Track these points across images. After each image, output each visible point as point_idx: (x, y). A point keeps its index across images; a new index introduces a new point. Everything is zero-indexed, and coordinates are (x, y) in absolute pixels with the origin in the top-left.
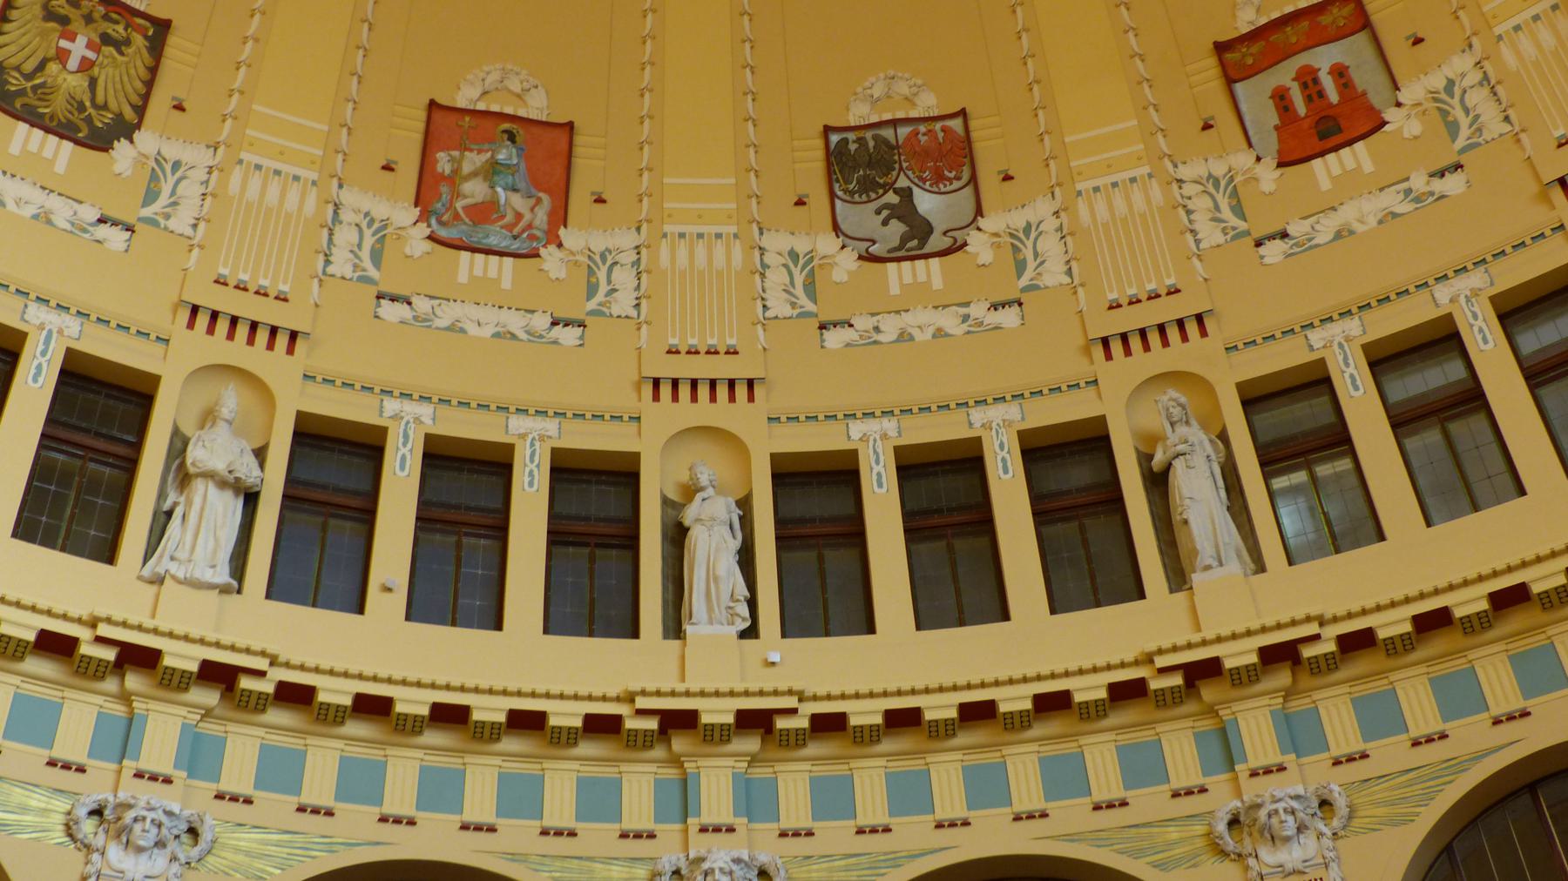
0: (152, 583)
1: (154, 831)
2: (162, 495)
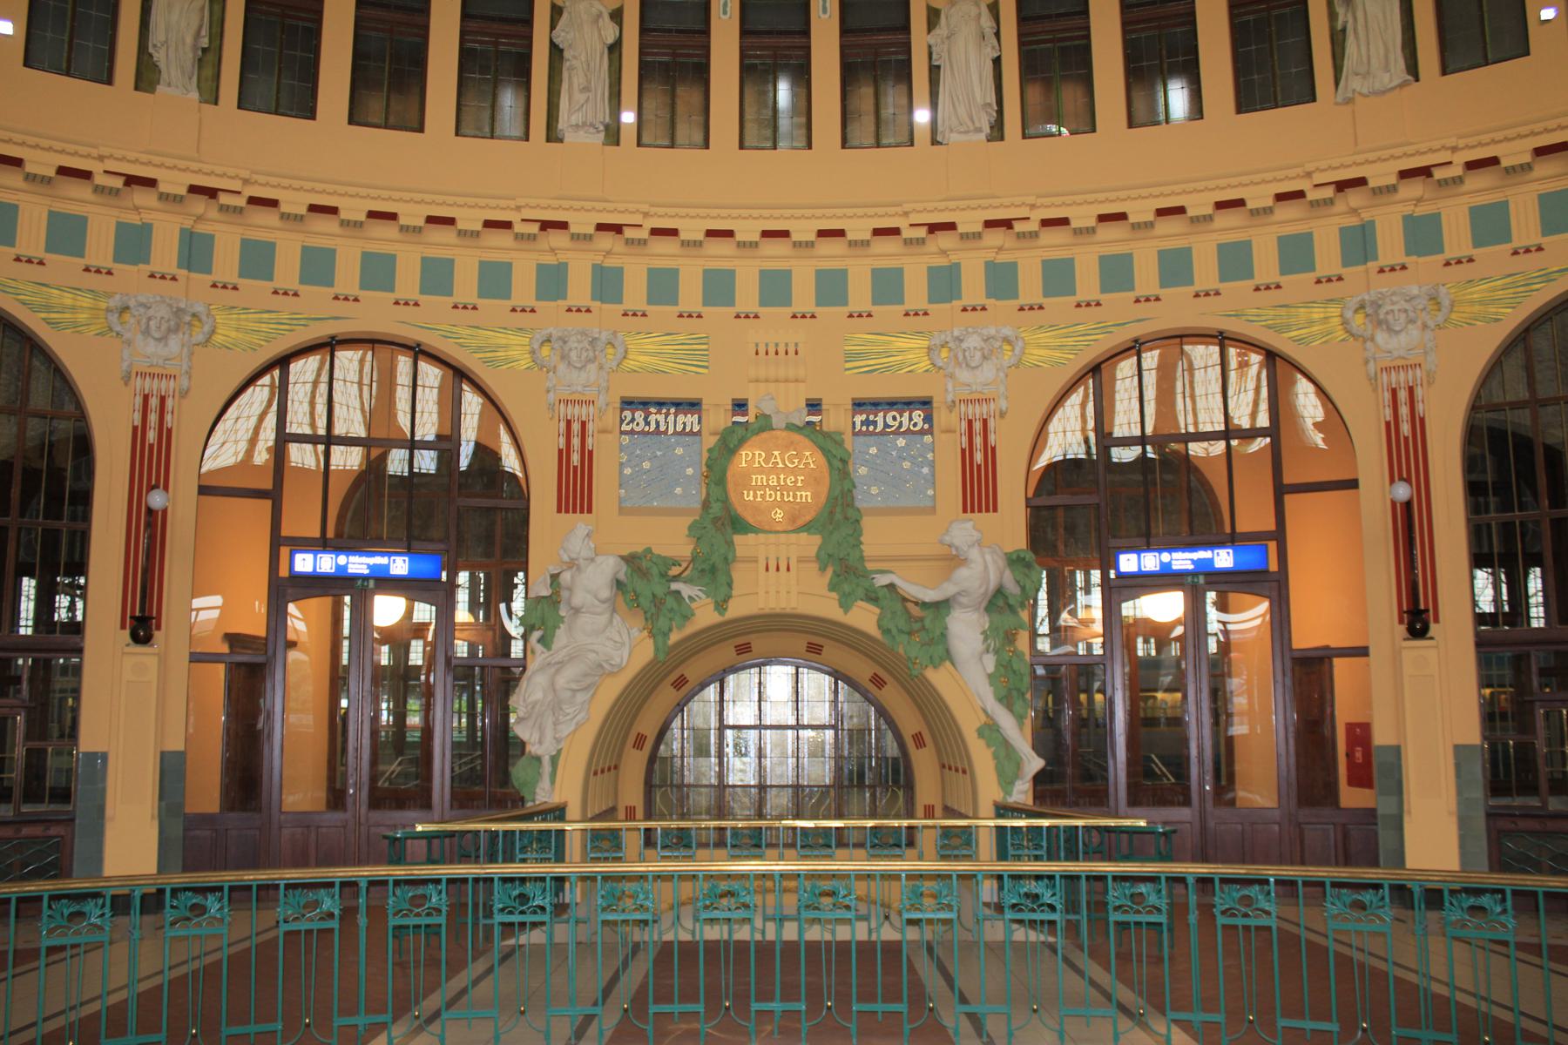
0: (1347, 103)
1: (1403, 316)
2: (1332, 16)
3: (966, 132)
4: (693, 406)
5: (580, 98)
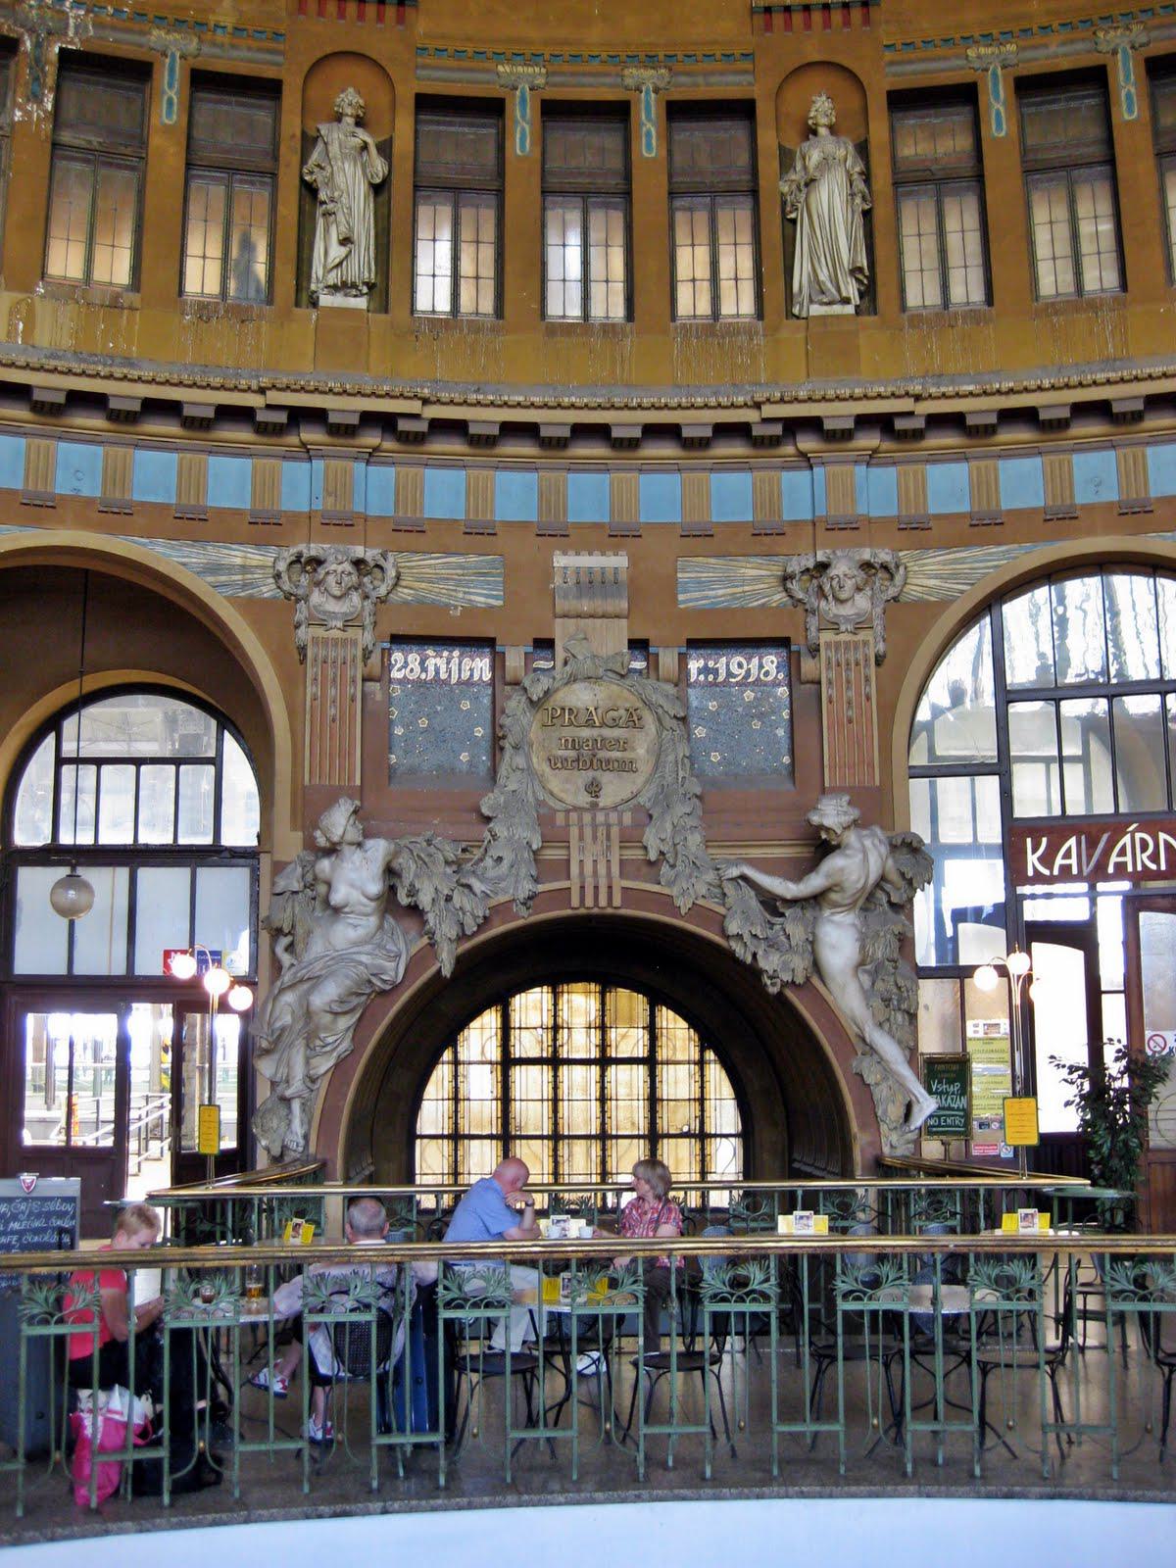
3: (829, 303)
5: (337, 252)
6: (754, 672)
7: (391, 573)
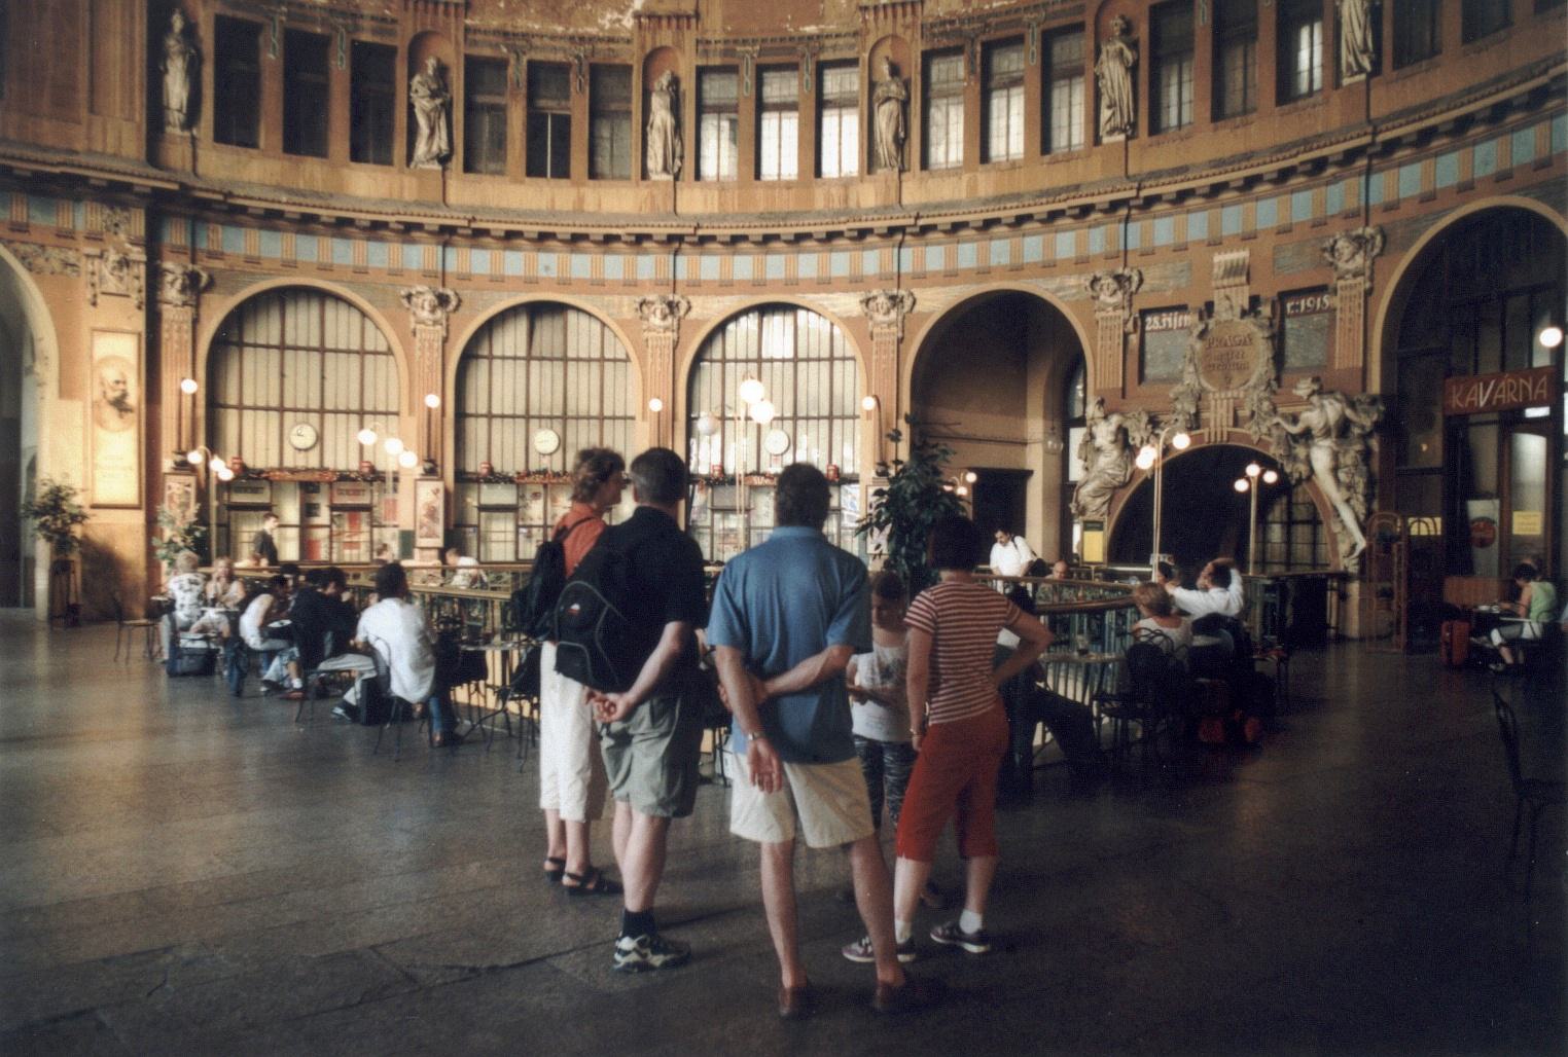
4: (1182, 308)
6: (1319, 305)
7: (1136, 278)
